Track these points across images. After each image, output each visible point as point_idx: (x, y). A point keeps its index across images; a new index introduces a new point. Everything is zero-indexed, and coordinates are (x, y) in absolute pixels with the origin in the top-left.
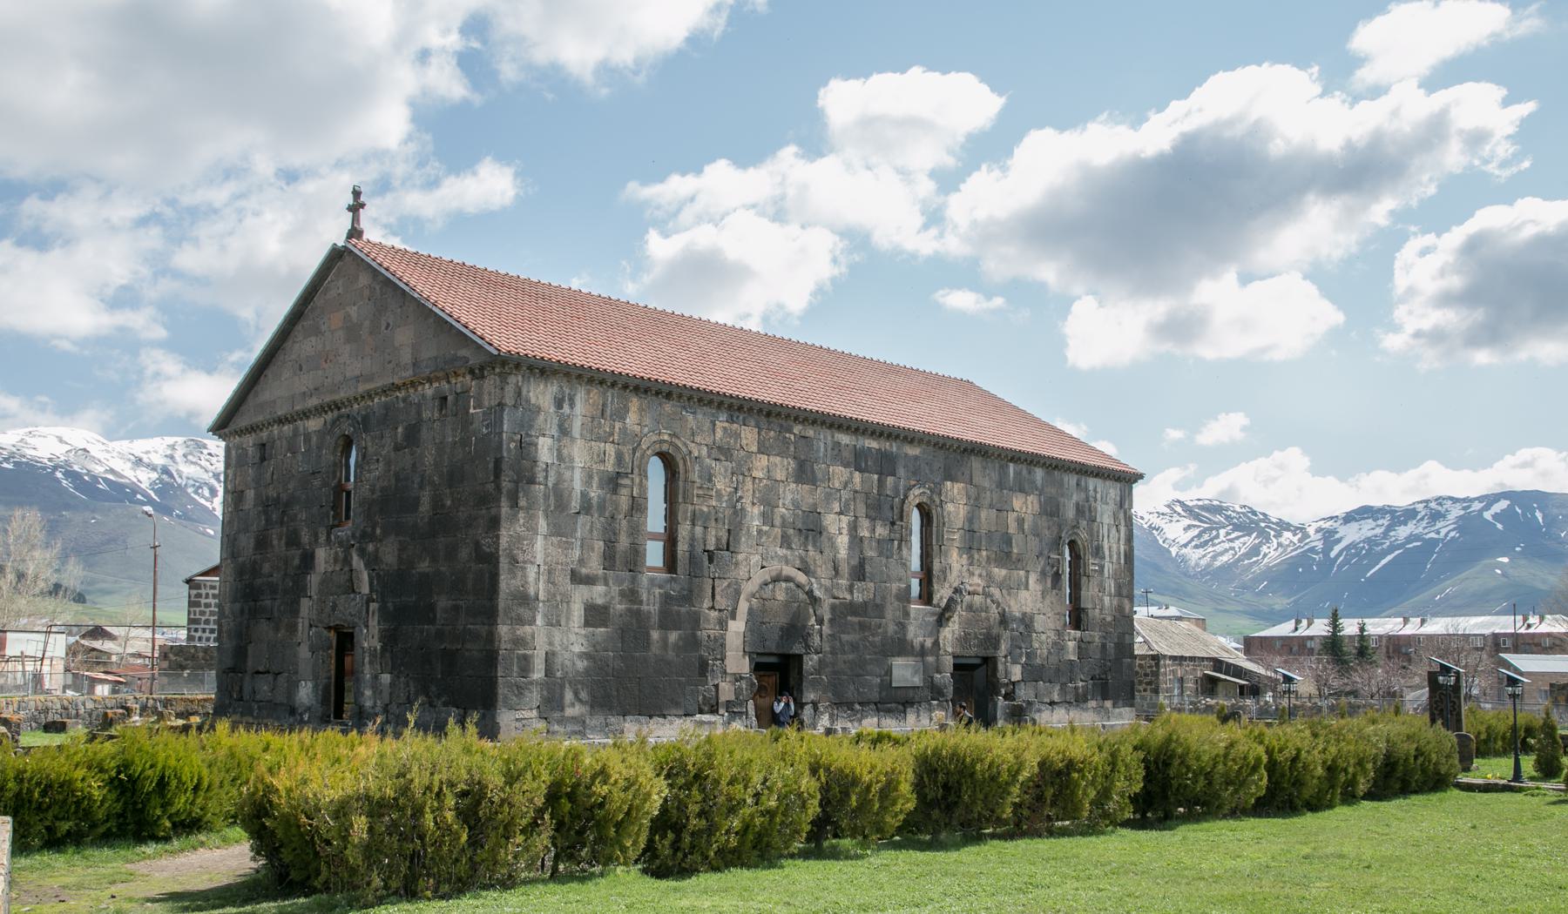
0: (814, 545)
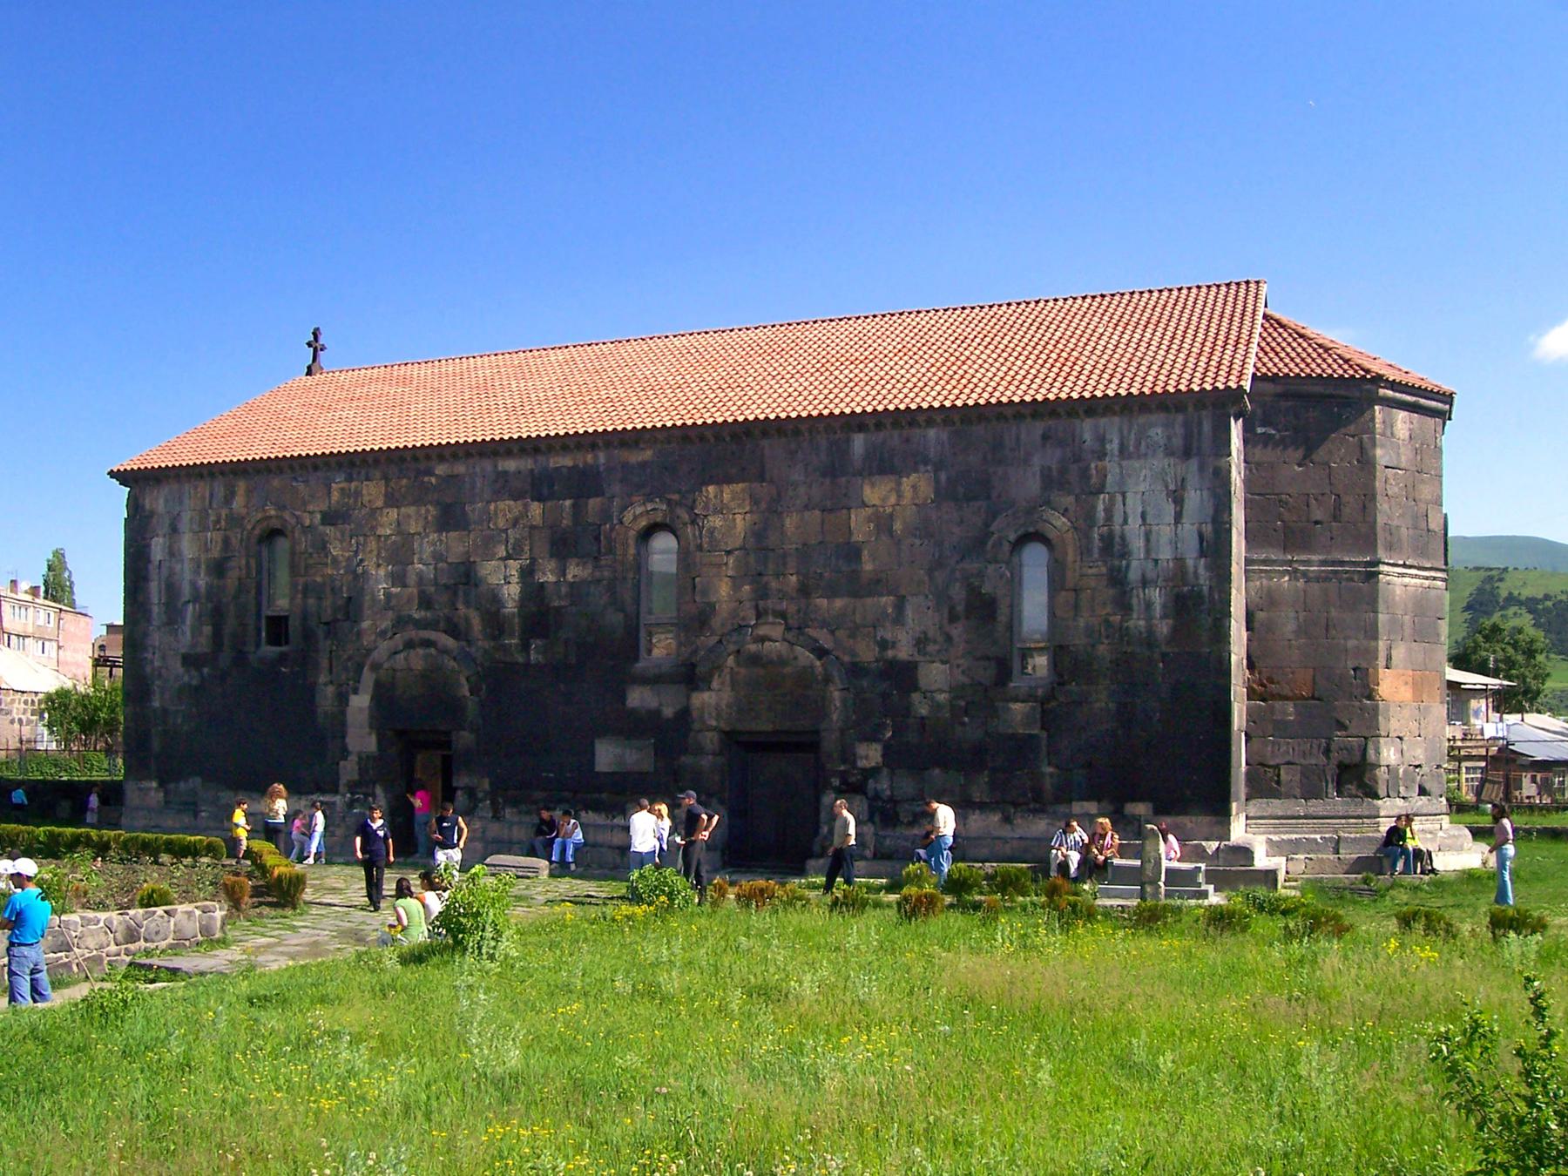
0: (467, 604)
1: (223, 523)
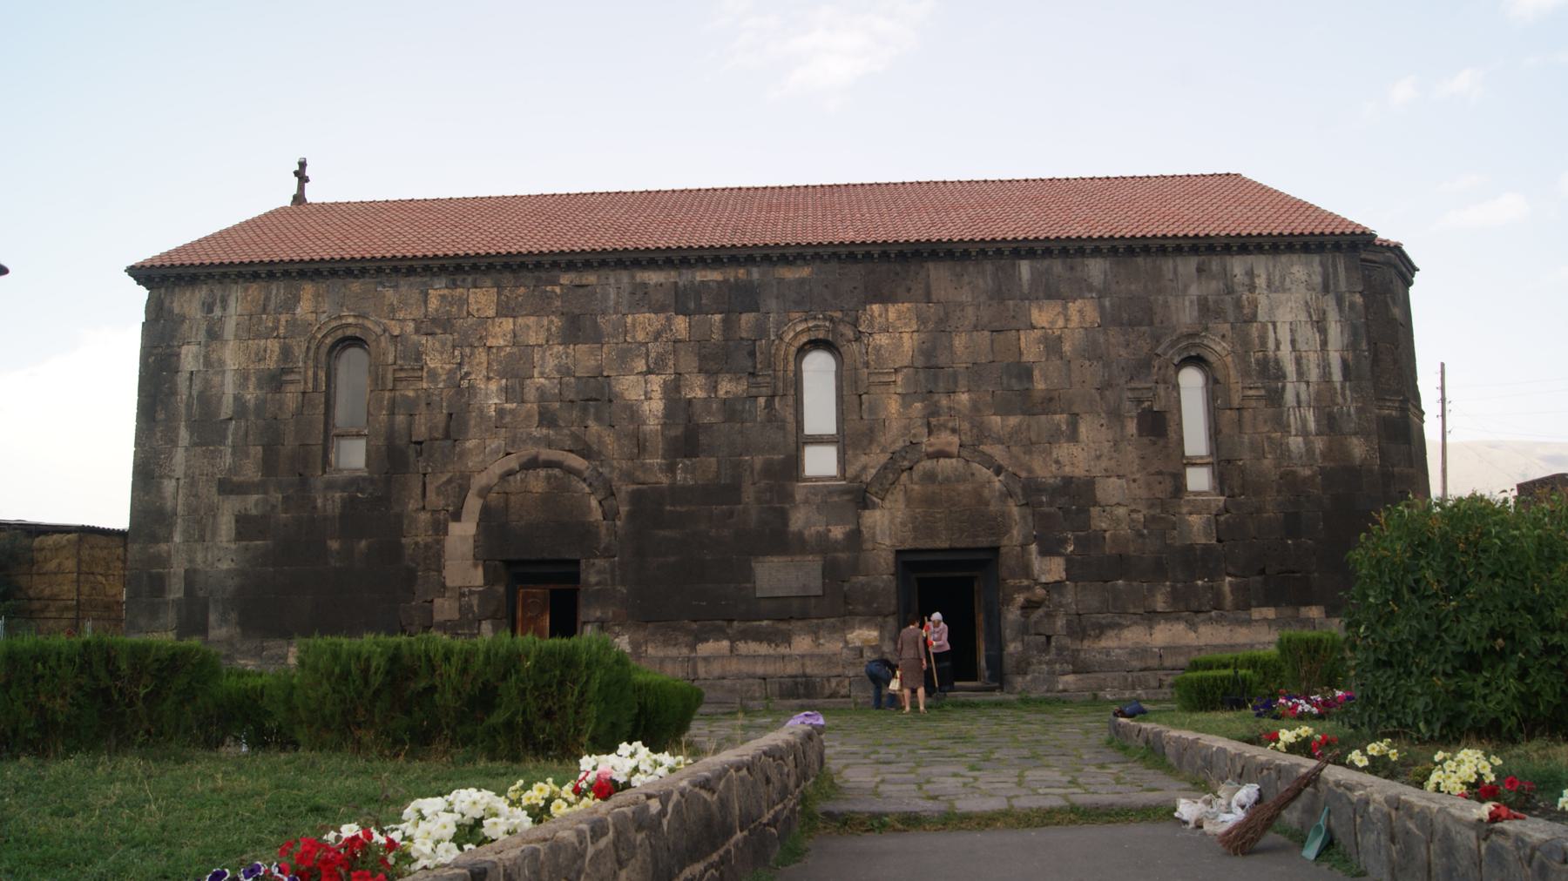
0: (599, 419)
1: (282, 331)
